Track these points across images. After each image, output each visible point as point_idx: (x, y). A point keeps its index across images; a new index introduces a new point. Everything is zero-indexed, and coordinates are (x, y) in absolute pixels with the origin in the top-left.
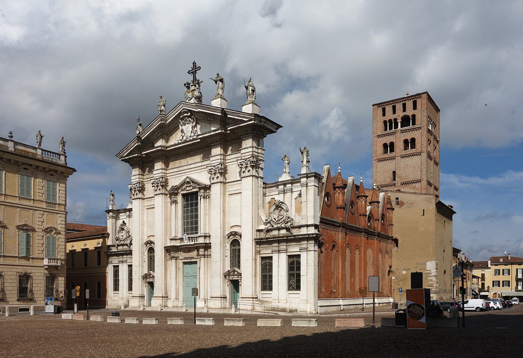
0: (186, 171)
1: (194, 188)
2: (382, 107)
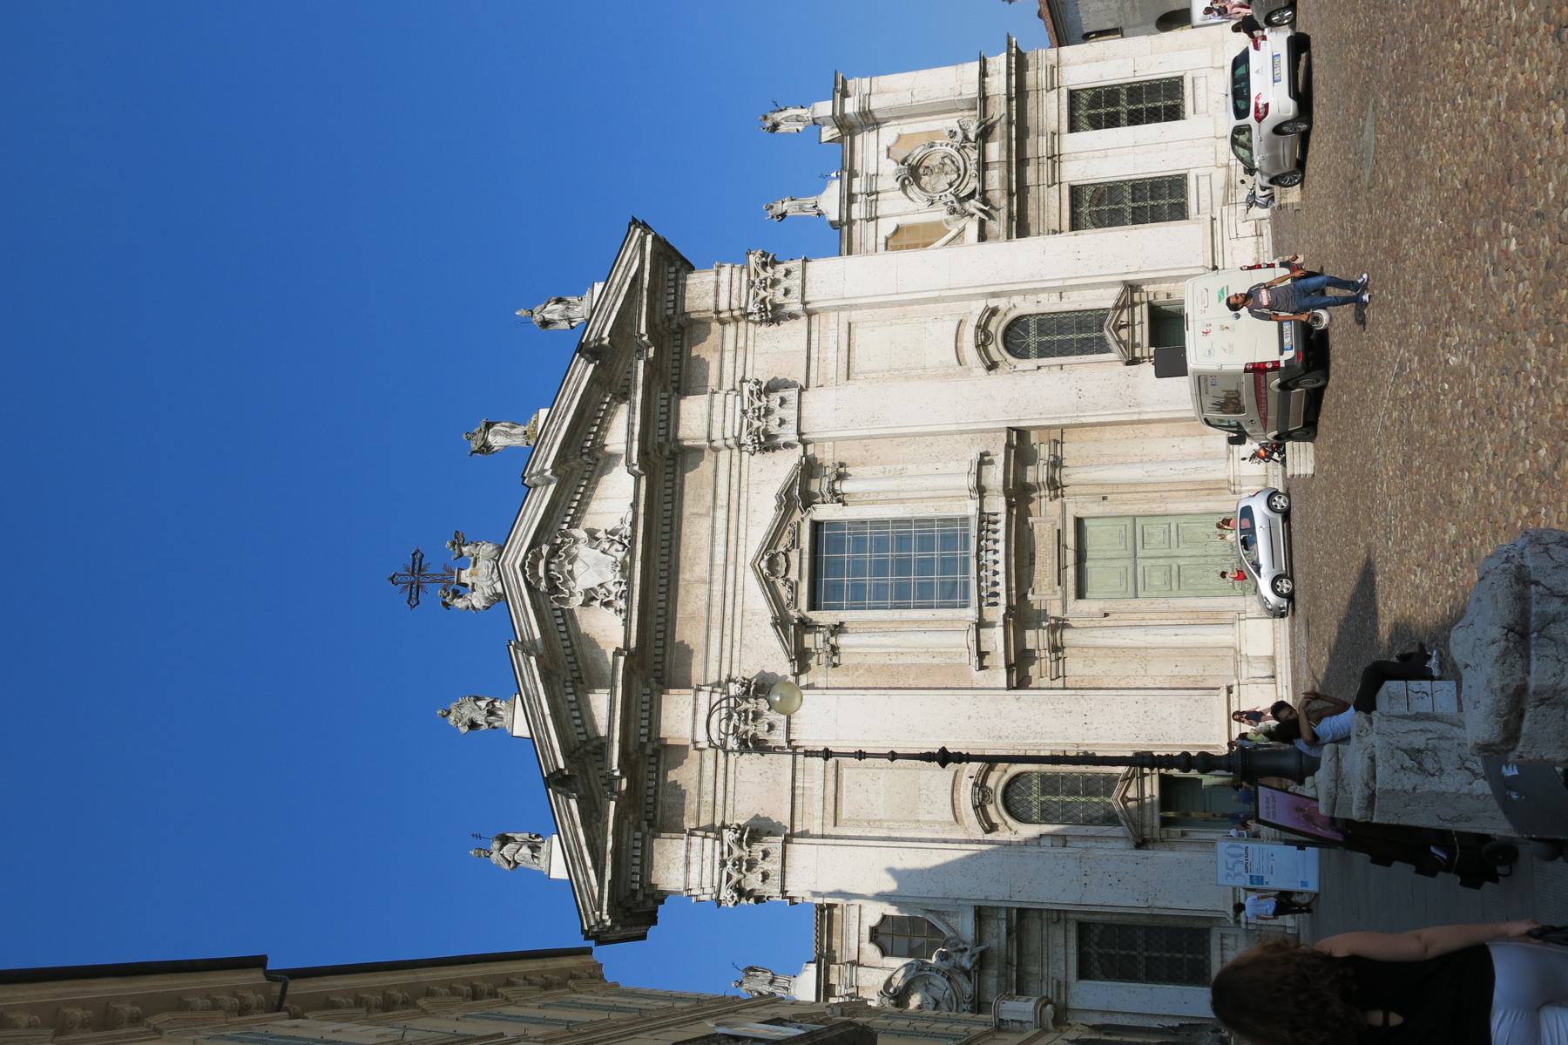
1: (797, 533)
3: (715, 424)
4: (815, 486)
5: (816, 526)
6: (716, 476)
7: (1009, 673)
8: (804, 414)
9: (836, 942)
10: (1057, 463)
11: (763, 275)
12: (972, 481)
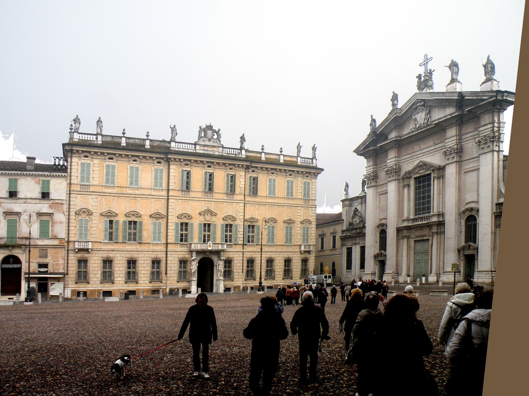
0: (418, 156)
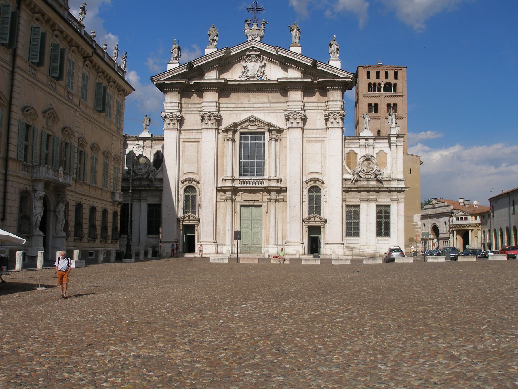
0: (246, 109)
1: (261, 128)
2: (367, 70)
3: (293, 103)
4: (274, 133)
5: (264, 133)
6: (279, 103)
7: (221, 187)
8: (294, 129)
9: (157, 142)
10: (276, 200)
11: (338, 115)
12: (272, 178)
